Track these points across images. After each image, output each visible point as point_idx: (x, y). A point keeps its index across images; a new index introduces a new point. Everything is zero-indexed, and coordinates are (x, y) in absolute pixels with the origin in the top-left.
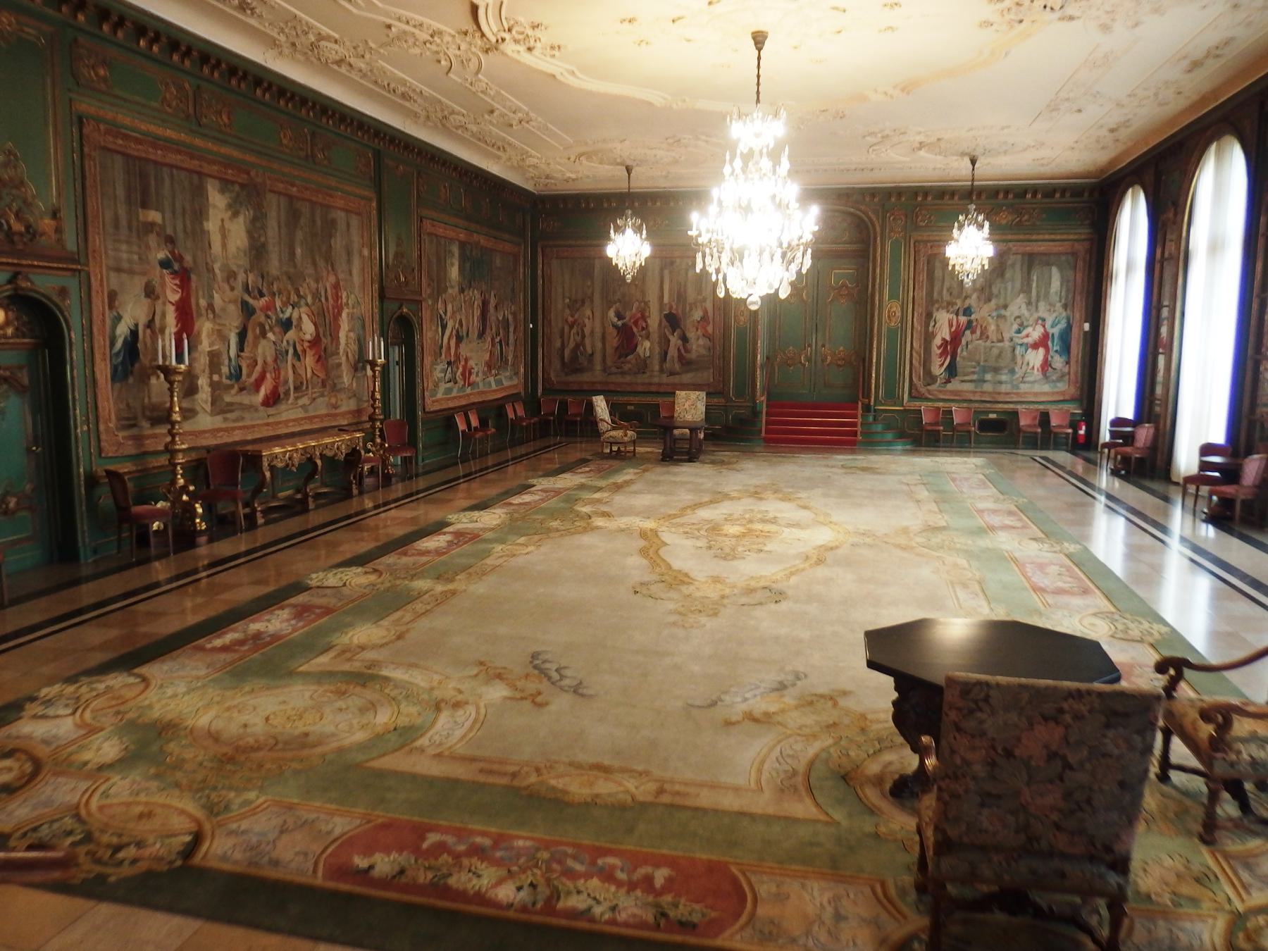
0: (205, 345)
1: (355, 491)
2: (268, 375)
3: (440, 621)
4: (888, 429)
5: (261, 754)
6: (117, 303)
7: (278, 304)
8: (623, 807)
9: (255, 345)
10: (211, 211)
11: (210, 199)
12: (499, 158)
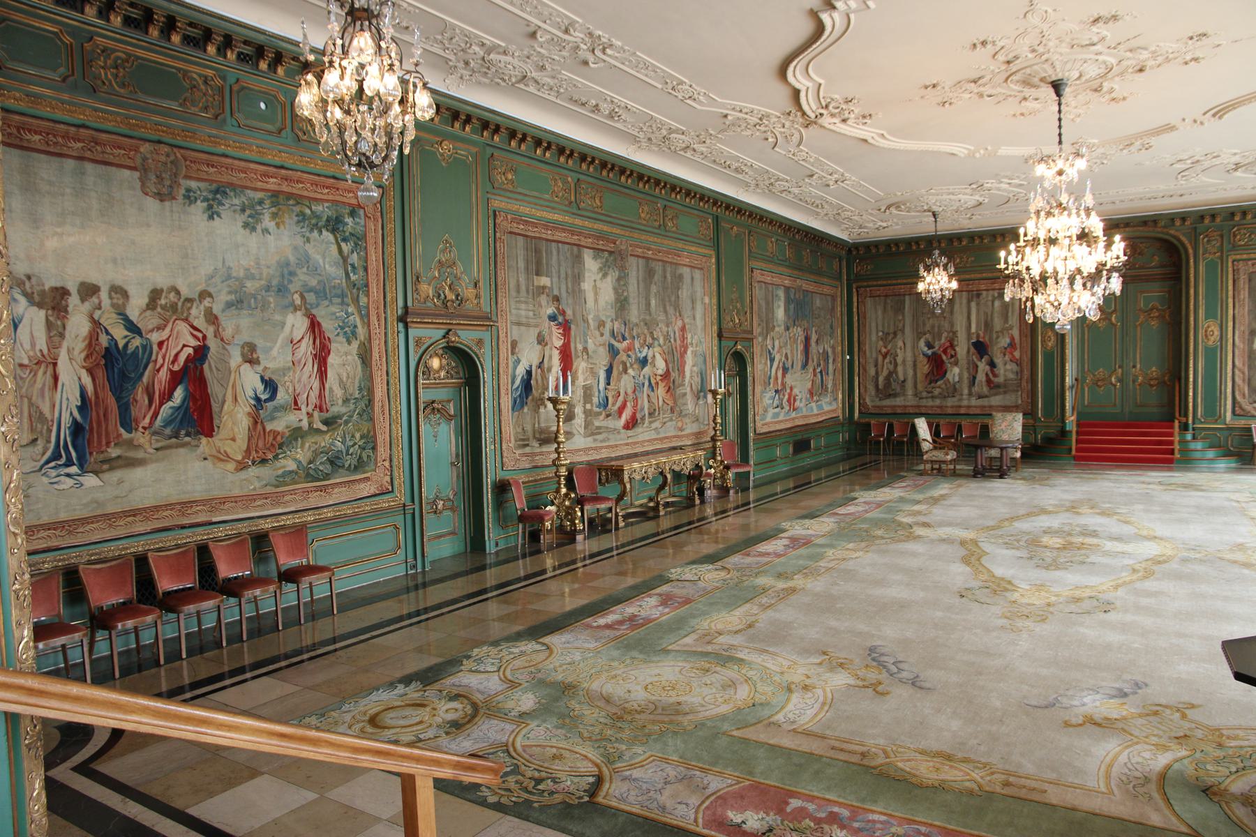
0: (581, 381)
1: (697, 502)
2: (628, 404)
3: (785, 613)
5: (643, 716)
7: (637, 345)
8: (971, 793)
10: (587, 275)
12: (818, 214)
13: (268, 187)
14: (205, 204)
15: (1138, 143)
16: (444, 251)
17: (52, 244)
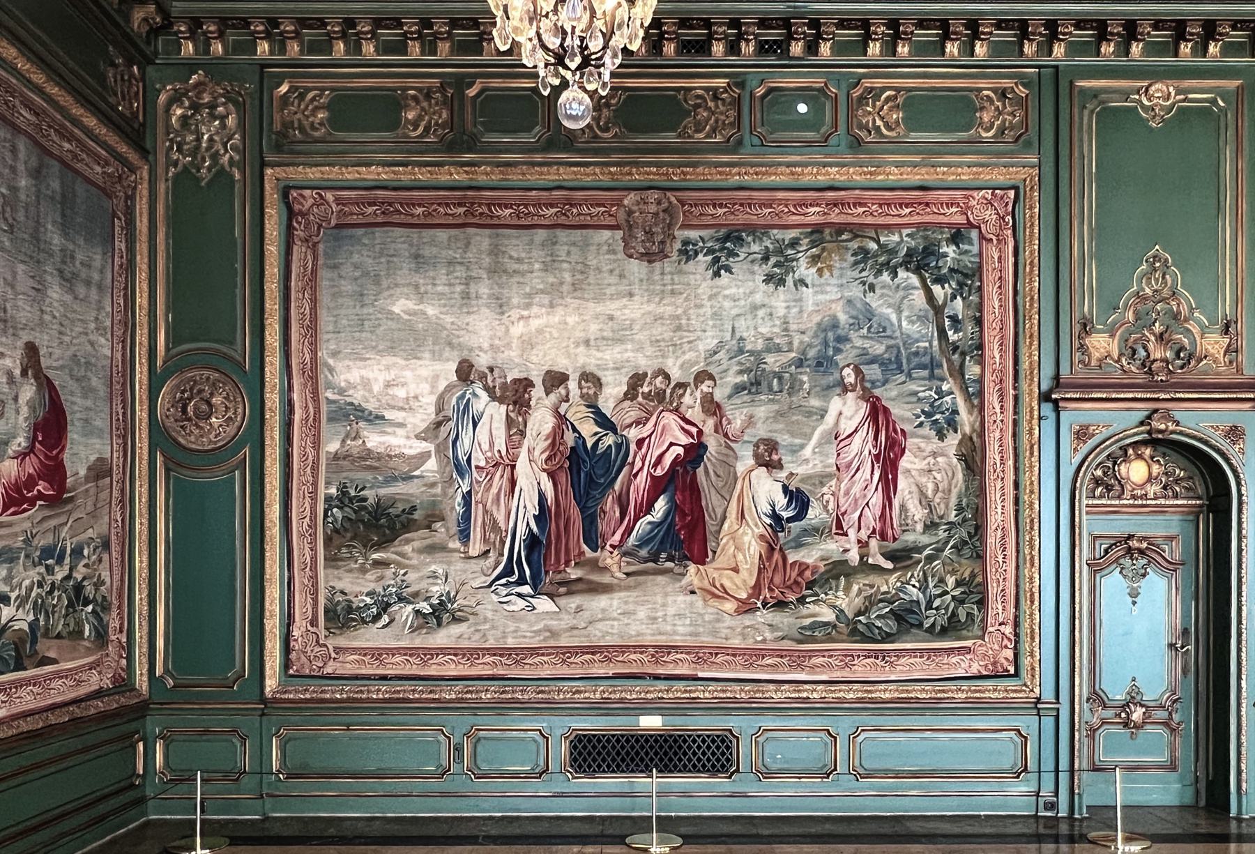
13: (808, 220)
14: (710, 258)
16: (1147, 275)
17: (518, 329)
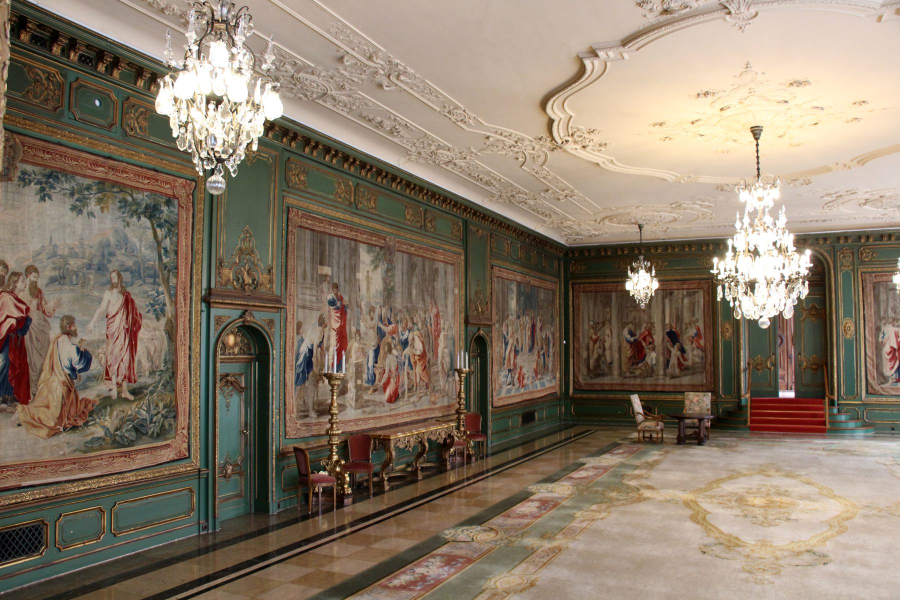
0: (353, 360)
2: (392, 380)
4: (851, 419)
6: (301, 330)
7: (400, 329)
9: (384, 359)
10: (361, 266)
11: (361, 258)
12: (545, 222)
13: (97, 174)
14: (38, 187)
15: (801, 180)
